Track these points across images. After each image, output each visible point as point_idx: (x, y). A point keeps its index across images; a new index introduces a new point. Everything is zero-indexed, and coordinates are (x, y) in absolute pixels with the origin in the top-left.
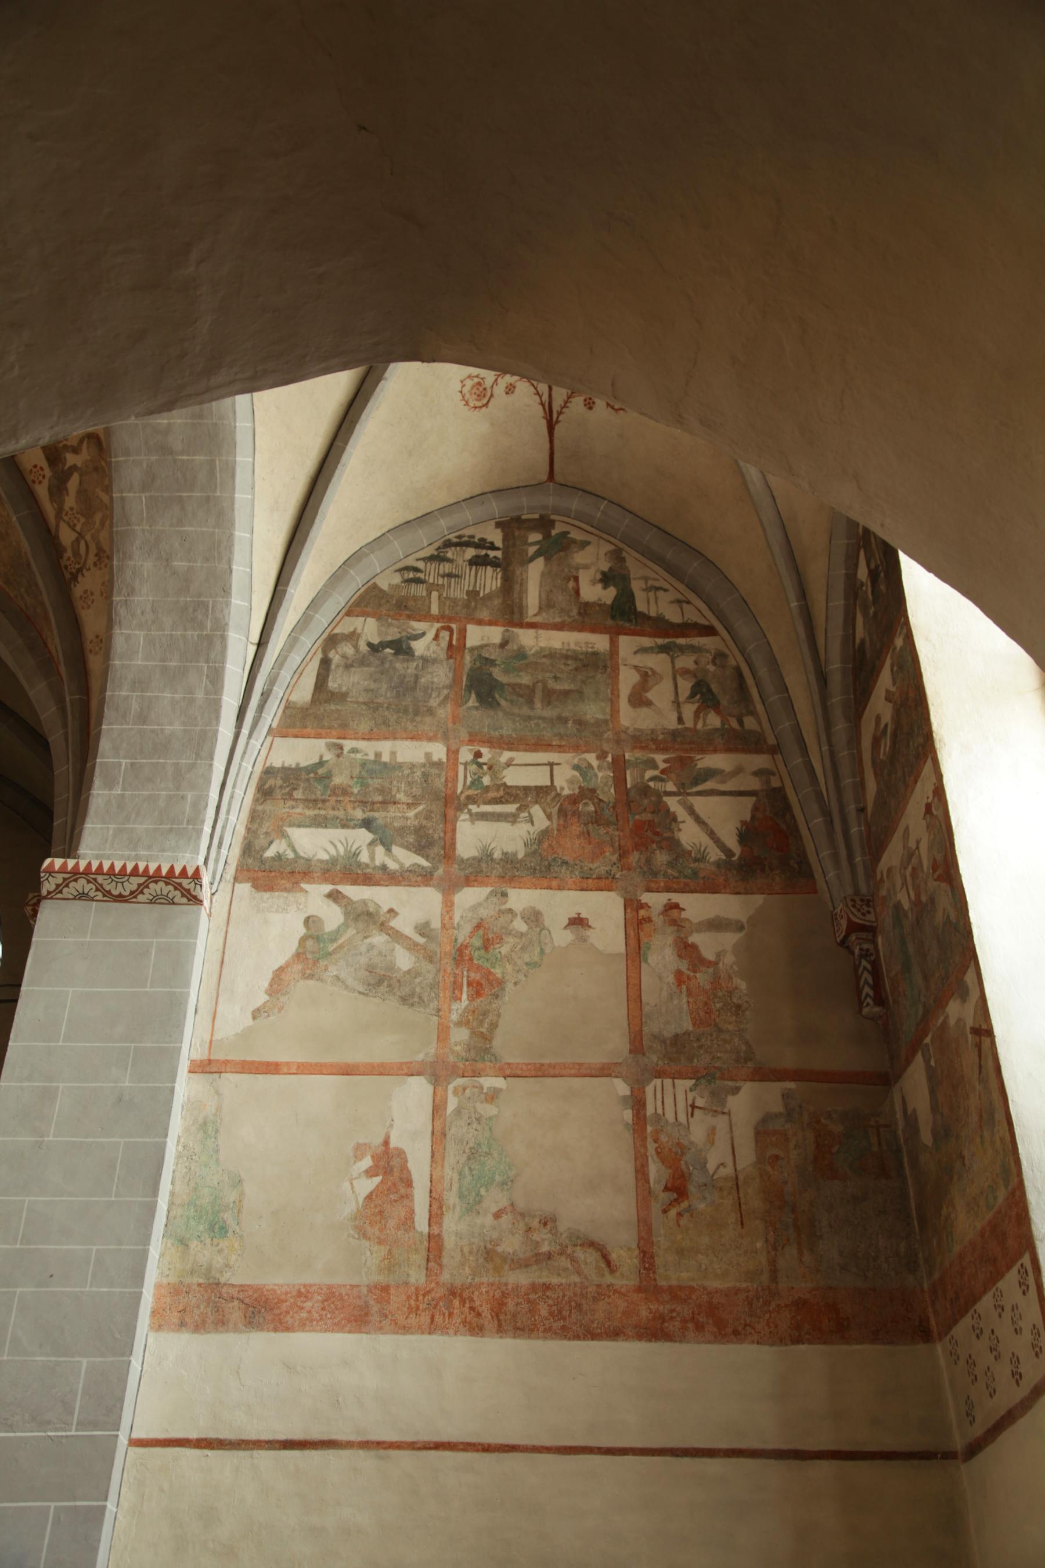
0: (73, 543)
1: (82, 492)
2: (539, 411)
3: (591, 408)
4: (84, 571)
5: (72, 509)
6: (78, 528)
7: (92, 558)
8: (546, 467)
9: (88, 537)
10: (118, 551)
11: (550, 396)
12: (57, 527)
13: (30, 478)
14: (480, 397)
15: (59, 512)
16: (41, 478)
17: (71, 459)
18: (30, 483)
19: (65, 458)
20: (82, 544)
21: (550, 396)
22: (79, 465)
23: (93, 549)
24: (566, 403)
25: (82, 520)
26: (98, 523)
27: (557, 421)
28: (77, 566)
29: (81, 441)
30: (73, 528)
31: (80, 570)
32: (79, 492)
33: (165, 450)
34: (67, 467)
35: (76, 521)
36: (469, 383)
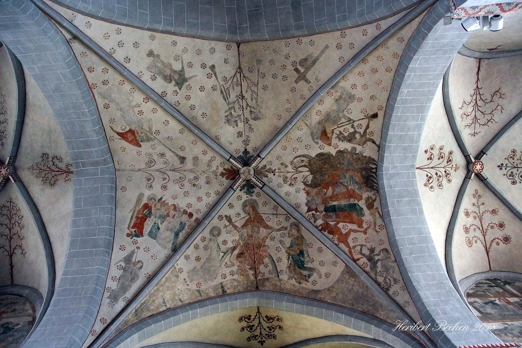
0: (383, 281)
1: (383, 266)
2: (483, 249)
3: (498, 245)
4: (391, 287)
5: (380, 271)
6: (384, 276)
7: (392, 283)
8: (489, 267)
9: (389, 277)
10: (409, 272)
11: (486, 243)
12: (376, 278)
13: (362, 267)
14: (470, 243)
15: (376, 274)
16: (367, 266)
17: (377, 258)
18: (363, 268)
19: (375, 258)
20: (387, 279)
21: (486, 243)
22: (380, 258)
23: (392, 280)
24: (490, 245)
25: (385, 273)
26: (391, 273)
27: (489, 251)
28: (387, 286)
29: (380, 252)
30: (382, 276)
31: (390, 287)
32: (382, 266)
33: (414, 244)
34: (376, 260)
35: (382, 274)
36: (467, 239)
